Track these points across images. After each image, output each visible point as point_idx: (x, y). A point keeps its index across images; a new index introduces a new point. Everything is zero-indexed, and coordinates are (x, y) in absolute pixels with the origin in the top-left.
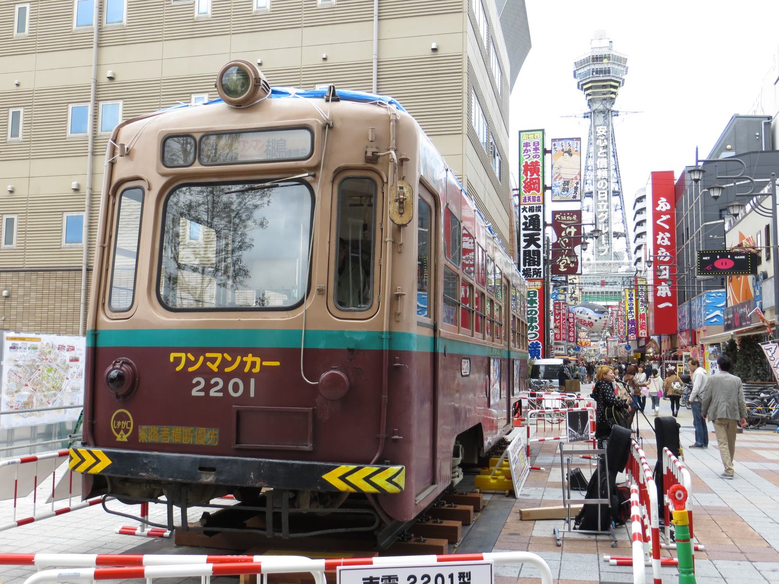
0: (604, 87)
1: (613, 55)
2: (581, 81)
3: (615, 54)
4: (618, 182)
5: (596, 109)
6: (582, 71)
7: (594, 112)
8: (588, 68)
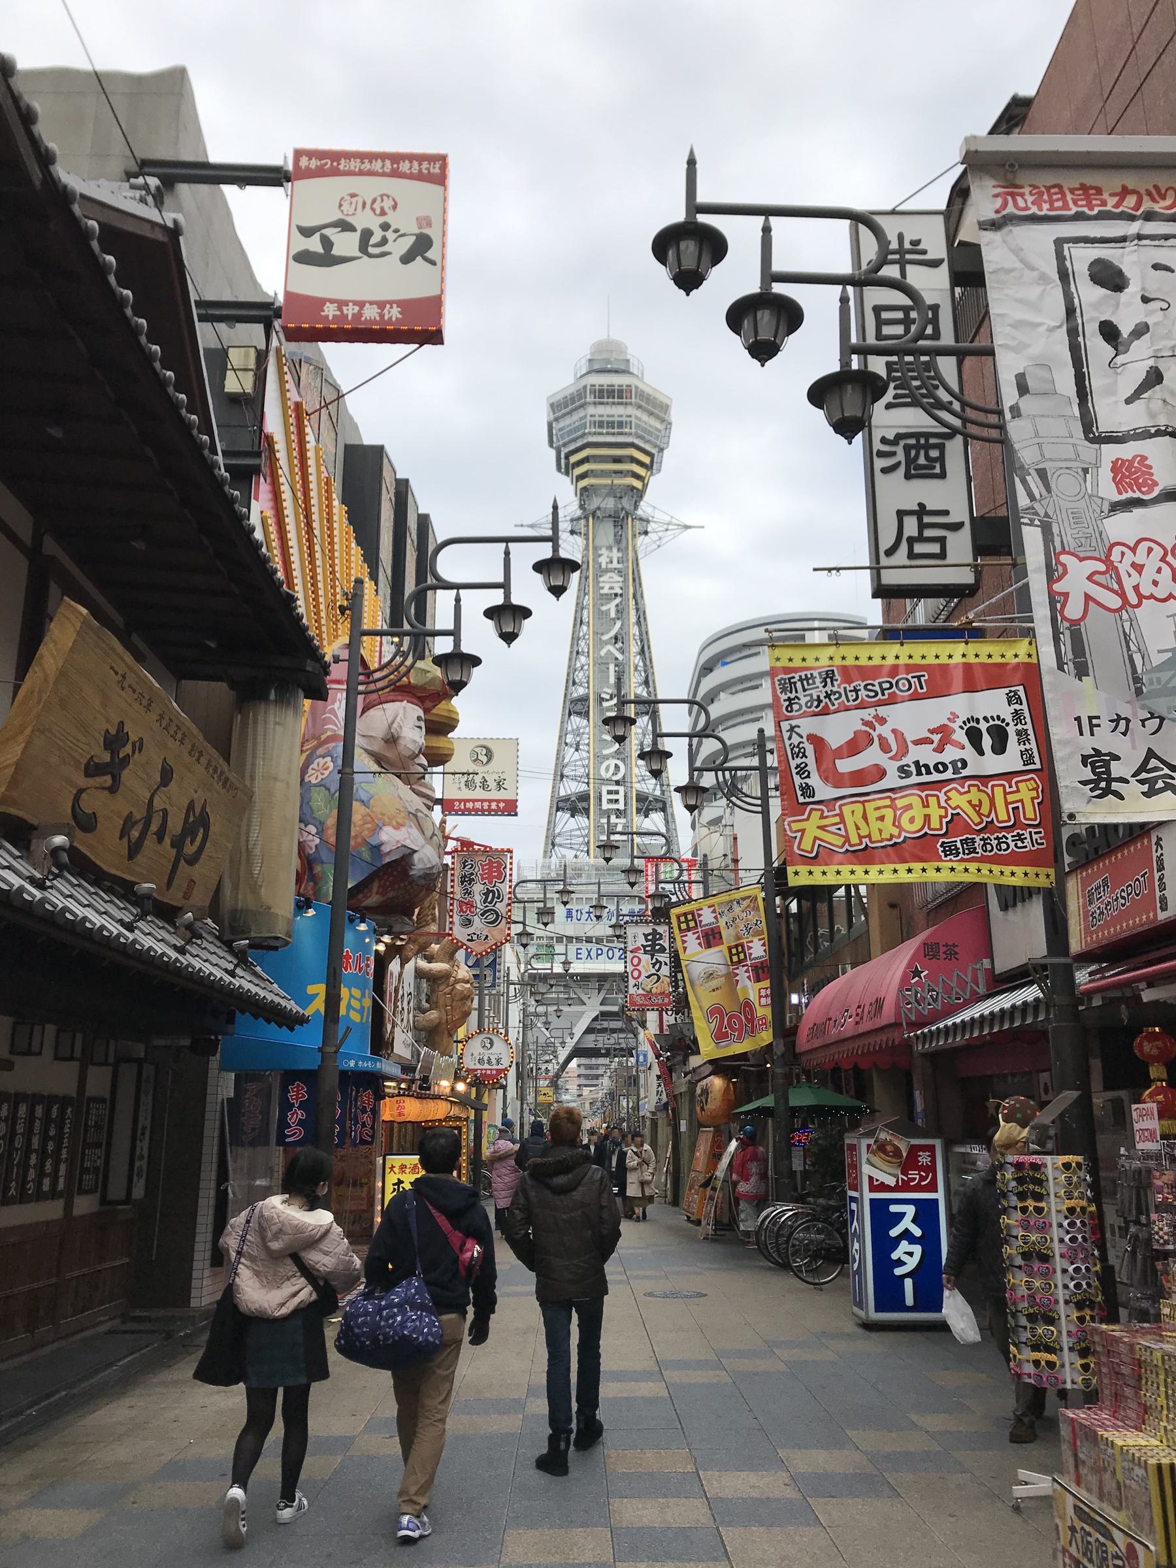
0: (617, 460)
1: (637, 388)
2: (565, 445)
3: (641, 386)
4: (646, 683)
5: (599, 508)
6: (567, 421)
7: (594, 514)
8: (581, 413)
